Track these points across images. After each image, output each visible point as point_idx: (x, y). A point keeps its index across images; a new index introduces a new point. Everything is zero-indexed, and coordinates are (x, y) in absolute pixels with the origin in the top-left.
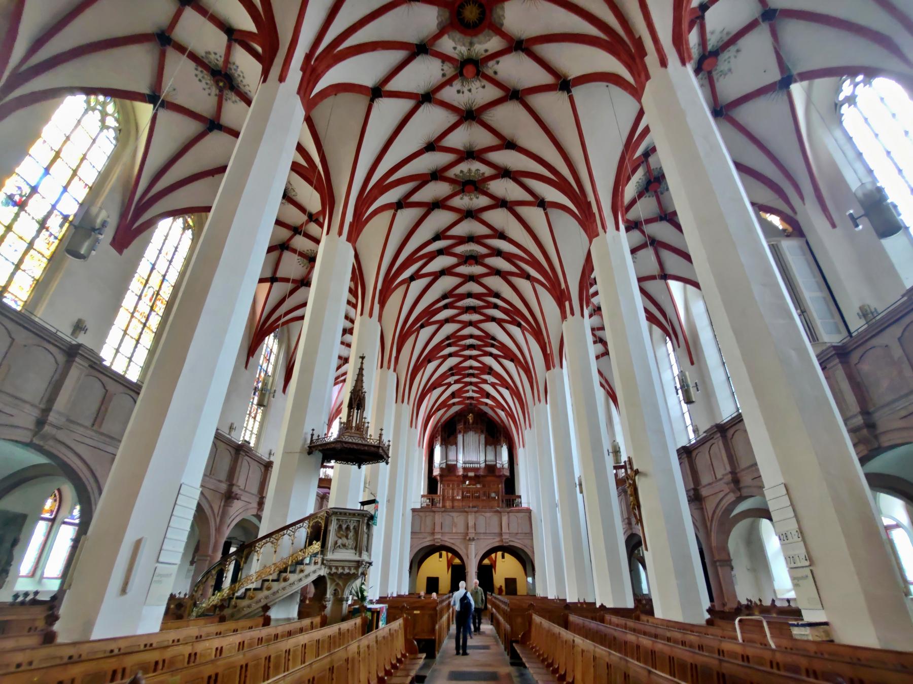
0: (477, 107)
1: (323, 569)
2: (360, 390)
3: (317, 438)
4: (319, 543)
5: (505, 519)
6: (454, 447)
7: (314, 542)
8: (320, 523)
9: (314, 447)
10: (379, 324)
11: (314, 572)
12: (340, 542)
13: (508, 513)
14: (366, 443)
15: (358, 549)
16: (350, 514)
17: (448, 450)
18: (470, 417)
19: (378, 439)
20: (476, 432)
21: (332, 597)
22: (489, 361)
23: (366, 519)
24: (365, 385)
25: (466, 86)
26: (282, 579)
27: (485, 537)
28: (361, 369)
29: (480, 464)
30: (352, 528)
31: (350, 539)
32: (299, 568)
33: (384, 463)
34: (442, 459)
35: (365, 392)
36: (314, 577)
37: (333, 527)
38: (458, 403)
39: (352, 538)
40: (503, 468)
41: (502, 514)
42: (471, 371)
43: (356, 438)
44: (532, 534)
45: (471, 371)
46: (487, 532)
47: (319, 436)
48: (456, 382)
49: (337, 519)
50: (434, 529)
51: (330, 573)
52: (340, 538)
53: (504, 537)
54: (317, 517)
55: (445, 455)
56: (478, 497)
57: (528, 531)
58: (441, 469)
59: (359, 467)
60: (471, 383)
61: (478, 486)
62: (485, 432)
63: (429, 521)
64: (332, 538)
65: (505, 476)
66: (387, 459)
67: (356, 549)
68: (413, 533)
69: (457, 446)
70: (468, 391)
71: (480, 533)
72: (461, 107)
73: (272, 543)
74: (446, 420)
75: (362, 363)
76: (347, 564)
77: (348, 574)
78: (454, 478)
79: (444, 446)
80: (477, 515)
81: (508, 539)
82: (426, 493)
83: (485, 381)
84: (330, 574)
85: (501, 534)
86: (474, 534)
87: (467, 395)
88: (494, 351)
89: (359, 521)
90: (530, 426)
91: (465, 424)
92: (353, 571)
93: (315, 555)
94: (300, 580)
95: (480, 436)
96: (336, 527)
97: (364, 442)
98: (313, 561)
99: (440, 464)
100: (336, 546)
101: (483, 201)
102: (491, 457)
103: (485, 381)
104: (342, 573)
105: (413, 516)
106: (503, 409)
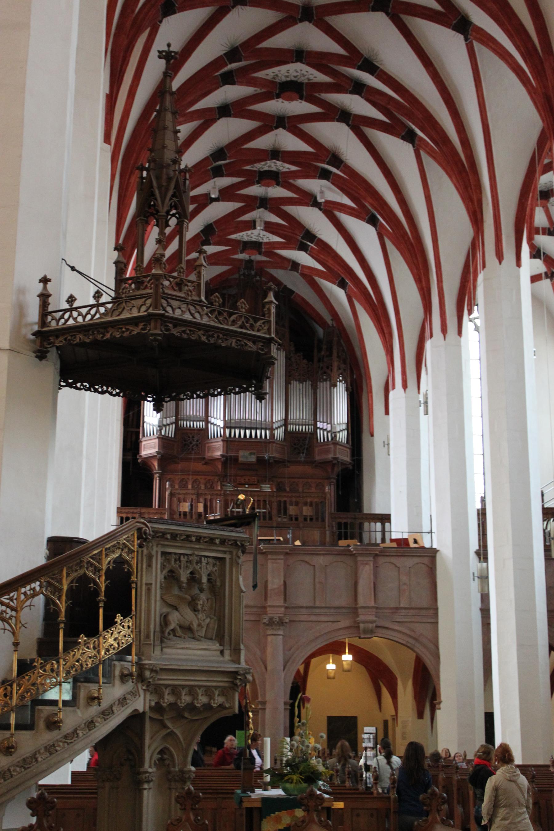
4: (129, 622)
8: (127, 562)
11: (122, 701)
12: (175, 618)
16: (199, 539)
26: (41, 724)
27: (313, 618)
29: (272, 430)
30: (205, 580)
40: (334, 442)
41: (359, 558)
44: (436, 609)
46: (317, 604)
49: (164, 554)
52: (175, 608)
53: (361, 618)
54: (116, 547)
58: (164, 441)
67: (220, 637)
70: (252, 225)
71: (301, 607)
76: (202, 680)
81: (372, 622)
84: (158, 708)
85: (354, 610)
86: (283, 609)
94: (90, 724)
98: (117, 673)
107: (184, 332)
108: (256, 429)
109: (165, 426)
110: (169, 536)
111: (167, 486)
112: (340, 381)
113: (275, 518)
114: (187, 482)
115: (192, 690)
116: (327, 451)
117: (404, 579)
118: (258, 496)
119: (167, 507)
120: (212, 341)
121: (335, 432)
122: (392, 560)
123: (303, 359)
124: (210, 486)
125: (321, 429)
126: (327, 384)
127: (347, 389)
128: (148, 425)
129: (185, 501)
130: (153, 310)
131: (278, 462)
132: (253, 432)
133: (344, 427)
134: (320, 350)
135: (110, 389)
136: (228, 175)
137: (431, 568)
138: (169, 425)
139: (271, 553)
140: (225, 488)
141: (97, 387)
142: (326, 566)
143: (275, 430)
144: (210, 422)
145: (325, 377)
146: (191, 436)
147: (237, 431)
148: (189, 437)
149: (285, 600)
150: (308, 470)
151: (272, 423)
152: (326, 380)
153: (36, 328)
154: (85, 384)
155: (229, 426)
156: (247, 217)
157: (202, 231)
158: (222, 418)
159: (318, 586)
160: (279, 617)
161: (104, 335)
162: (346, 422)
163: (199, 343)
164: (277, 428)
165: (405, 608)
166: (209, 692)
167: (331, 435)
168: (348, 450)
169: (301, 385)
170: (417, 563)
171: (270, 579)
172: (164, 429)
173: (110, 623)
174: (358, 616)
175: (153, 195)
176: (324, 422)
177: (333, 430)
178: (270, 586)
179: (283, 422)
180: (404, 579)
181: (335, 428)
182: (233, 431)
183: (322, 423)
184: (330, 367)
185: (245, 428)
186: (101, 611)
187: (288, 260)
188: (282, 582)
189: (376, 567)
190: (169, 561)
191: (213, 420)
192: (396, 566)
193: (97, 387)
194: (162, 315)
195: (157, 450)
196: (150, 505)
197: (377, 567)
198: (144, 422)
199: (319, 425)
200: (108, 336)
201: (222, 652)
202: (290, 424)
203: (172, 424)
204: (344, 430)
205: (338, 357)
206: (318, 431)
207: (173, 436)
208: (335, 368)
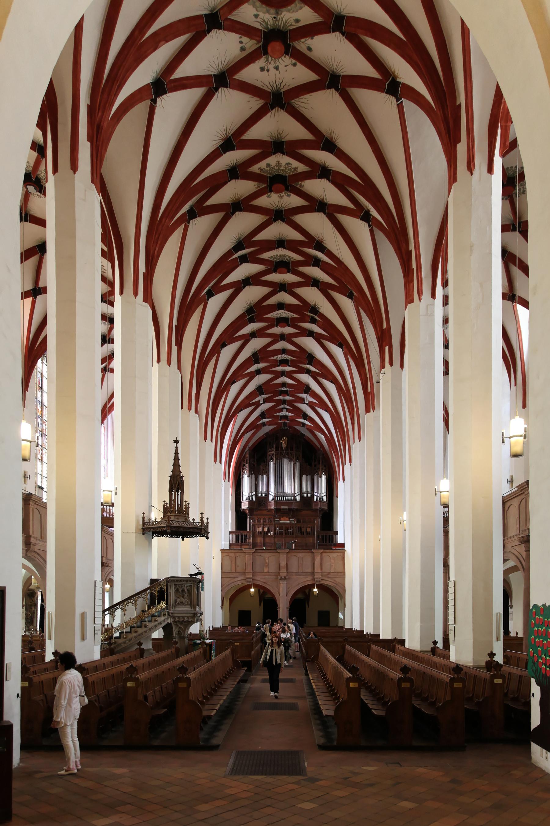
0: (286, 88)
1: (170, 618)
6: (264, 477)
7: (161, 602)
8: (164, 589)
9: (147, 529)
11: (164, 621)
12: (178, 600)
14: (191, 526)
15: (191, 604)
16: (184, 581)
18: (284, 441)
19: (200, 522)
20: (291, 459)
21: (177, 635)
22: (305, 378)
23: (196, 583)
25: (273, 62)
29: (294, 497)
30: (186, 591)
31: (186, 598)
32: (153, 618)
34: (251, 492)
35: (183, 476)
36: (164, 624)
37: (172, 591)
39: (187, 597)
43: (182, 522)
49: (174, 585)
51: (174, 621)
52: (179, 598)
54: (160, 585)
55: (254, 486)
58: (251, 502)
59: (183, 540)
64: (172, 597)
67: (191, 604)
69: (268, 476)
72: (265, 88)
73: (132, 603)
77: (188, 621)
78: (266, 512)
79: (253, 476)
82: (234, 530)
84: (174, 622)
89: (191, 585)
90: (360, 438)
91: (277, 449)
92: (190, 619)
93: (163, 610)
96: (174, 590)
97: (189, 526)
98: (162, 614)
99: (249, 497)
100: (176, 604)
101: (295, 201)
102: (307, 488)
104: (183, 621)
106: (323, 432)
109: (251, 496)
112: (323, 475)
113: (294, 534)
115: (183, 617)
118: (288, 525)
120: (185, 530)
124: (270, 521)
129: (260, 527)
133: (325, 494)
137: (343, 557)
139: (282, 553)
152: (317, 475)
153: (142, 527)
166: (188, 618)
173: (159, 603)
179: (299, 493)
182: (278, 498)
184: (318, 469)
186: (157, 600)
190: (176, 586)
198: (242, 495)
199: (315, 494)
200: (158, 530)
201: (191, 608)
203: (254, 495)
205: (322, 464)
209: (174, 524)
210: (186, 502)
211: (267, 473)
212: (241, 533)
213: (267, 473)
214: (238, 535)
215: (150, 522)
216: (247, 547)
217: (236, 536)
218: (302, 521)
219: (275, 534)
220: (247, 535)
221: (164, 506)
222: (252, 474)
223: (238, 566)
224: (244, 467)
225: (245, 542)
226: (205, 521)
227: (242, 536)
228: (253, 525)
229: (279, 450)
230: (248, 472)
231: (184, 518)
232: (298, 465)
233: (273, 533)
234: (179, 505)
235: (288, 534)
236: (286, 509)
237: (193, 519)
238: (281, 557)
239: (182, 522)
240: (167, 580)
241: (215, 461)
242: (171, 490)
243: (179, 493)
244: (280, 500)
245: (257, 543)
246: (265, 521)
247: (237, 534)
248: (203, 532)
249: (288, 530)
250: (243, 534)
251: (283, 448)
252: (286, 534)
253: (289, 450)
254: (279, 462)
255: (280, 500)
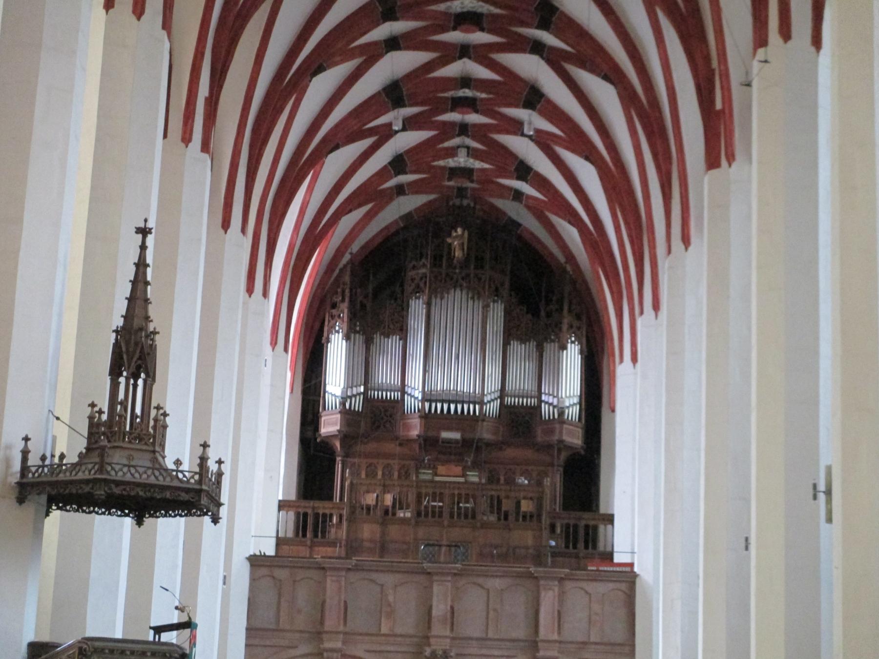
2: (141, 329)
3: (41, 463)
5: (548, 599)
6: (393, 343)
10: (164, 33)
13: (561, 580)
17: (373, 348)
19: (197, 470)
20: (476, 293)
24: (152, 311)
27: (484, 651)
28: (141, 265)
29: (482, 403)
33: (207, 519)
34: (350, 383)
38: (416, 188)
41: (542, 582)
42: (467, 93)
43: (141, 470)
44: (633, 646)
45: (467, 93)
46: (491, 635)
47: (43, 458)
48: (409, 124)
50: (322, 623)
56: (471, 515)
57: (619, 636)
58: (348, 415)
60: (464, 129)
61: (473, 477)
62: (505, 292)
63: (303, 595)
65: (569, 447)
66: (216, 509)
68: (251, 631)
70: (452, 152)
71: (471, 639)
74: (367, 244)
75: (143, 247)
79: (359, 339)
80: (462, 582)
82: (293, 496)
83: (516, 127)
87: (451, 163)
88: (549, 39)
91: (437, 260)
95: (486, 307)
103: (516, 127)
105: (253, 580)
107: (124, 490)
108: (463, 402)
109: (350, 397)
110: (107, 651)
111: (347, 475)
112: (572, 342)
113: (479, 517)
114: (376, 467)
116: (552, 432)
117: (596, 607)
118: (459, 488)
119: (346, 500)
120: (149, 494)
121: (563, 408)
122: (584, 585)
123: (527, 313)
125: (546, 403)
126: (555, 346)
127: (581, 352)
128: (330, 396)
129: (374, 492)
130: (99, 474)
131: (488, 444)
132: (459, 407)
134: (548, 302)
135: (96, 509)
136: (411, 105)
138: (355, 396)
139: (437, 574)
140: (422, 477)
141: (85, 508)
142: (502, 590)
143: (486, 404)
144: (407, 393)
145: (553, 337)
146: (383, 410)
147: (439, 405)
148: (380, 411)
149: (452, 630)
150: (529, 454)
151: (483, 394)
152: (553, 341)
154: (74, 506)
155: (429, 398)
156: (446, 144)
157: (390, 163)
158: (420, 389)
159: (491, 613)
160: (442, 650)
161: (65, 490)
162: (579, 394)
163: (137, 496)
164: (489, 402)
165: (596, 644)
167: (558, 410)
168: (580, 430)
169: (523, 345)
170: (613, 590)
171: (434, 604)
172: (349, 401)
174: (538, 651)
175: (122, 358)
176: (550, 395)
177: (560, 405)
178: (435, 612)
179: (497, 394)
180: (596, 607)
181: (563, 402)
182: (433, 405)
183: (547, 396)
184: (558, 325)
185: (449, 402)
187: (510, 189)
188: (449, 608)
189: (562, 594)
191: (409, 391)
192: (587, 592)
193: (85, 508)
194: (105, 480)
195: (338, 428)
196: (330, 498)
197: (563, 592)
199: (544, 397)
200: (67, 491)
202: (508, 396)
203: (359, 394)
204: (574, 404)
205: (570, 311)
206: (543, 405)
207: (360, 410)
208: (565, 327)
209: (116, 473)
210: (158, 408)
211: (401, 330)
212: (314, 508)
213: (401, 330)
214: (305, 515)
215: (43, 466)
216: (329, 550)
217: (298, 515)
218: (502, 478)
219: (419, 514)
220: (331, 515)
221: (91, 418)
222: (358, 332)
223: (299, 611)
224: (334, 312)
225: (323, 536)
226: (213, 466)
227: (317, 515)
228: (352, 484)
229: (441, 266)
230: (345, 326)
231: (149, 456)
232: (497, 311)
233: (412, 512)
234: (137, 417)
235: (459, 515)
236: (456, 441)
237: (178, 462)
238: (436, 588)
239: (141, 470)
240: (80, 649)
241: (250, 290)
242: (115, 372)
243: (140, 382)
244: (439, 412)
245: (363, 540)
246: (391, 475)
247: (301, 511)
248: (204, 501)
249: (458, 503)
250: (321, 512)
251: (453, 259)
252: (452, 516)
253: (472, 267)
254: (438, 300)
255: (439, 412)
